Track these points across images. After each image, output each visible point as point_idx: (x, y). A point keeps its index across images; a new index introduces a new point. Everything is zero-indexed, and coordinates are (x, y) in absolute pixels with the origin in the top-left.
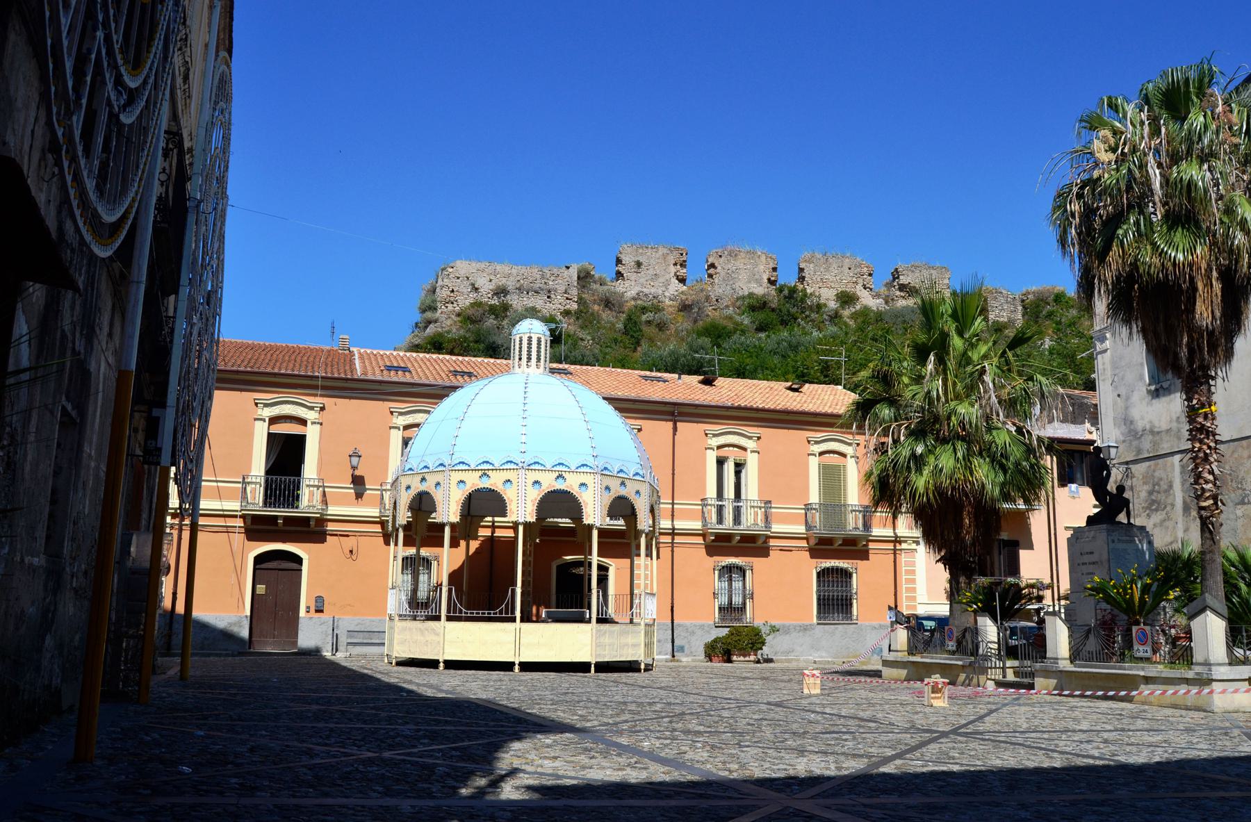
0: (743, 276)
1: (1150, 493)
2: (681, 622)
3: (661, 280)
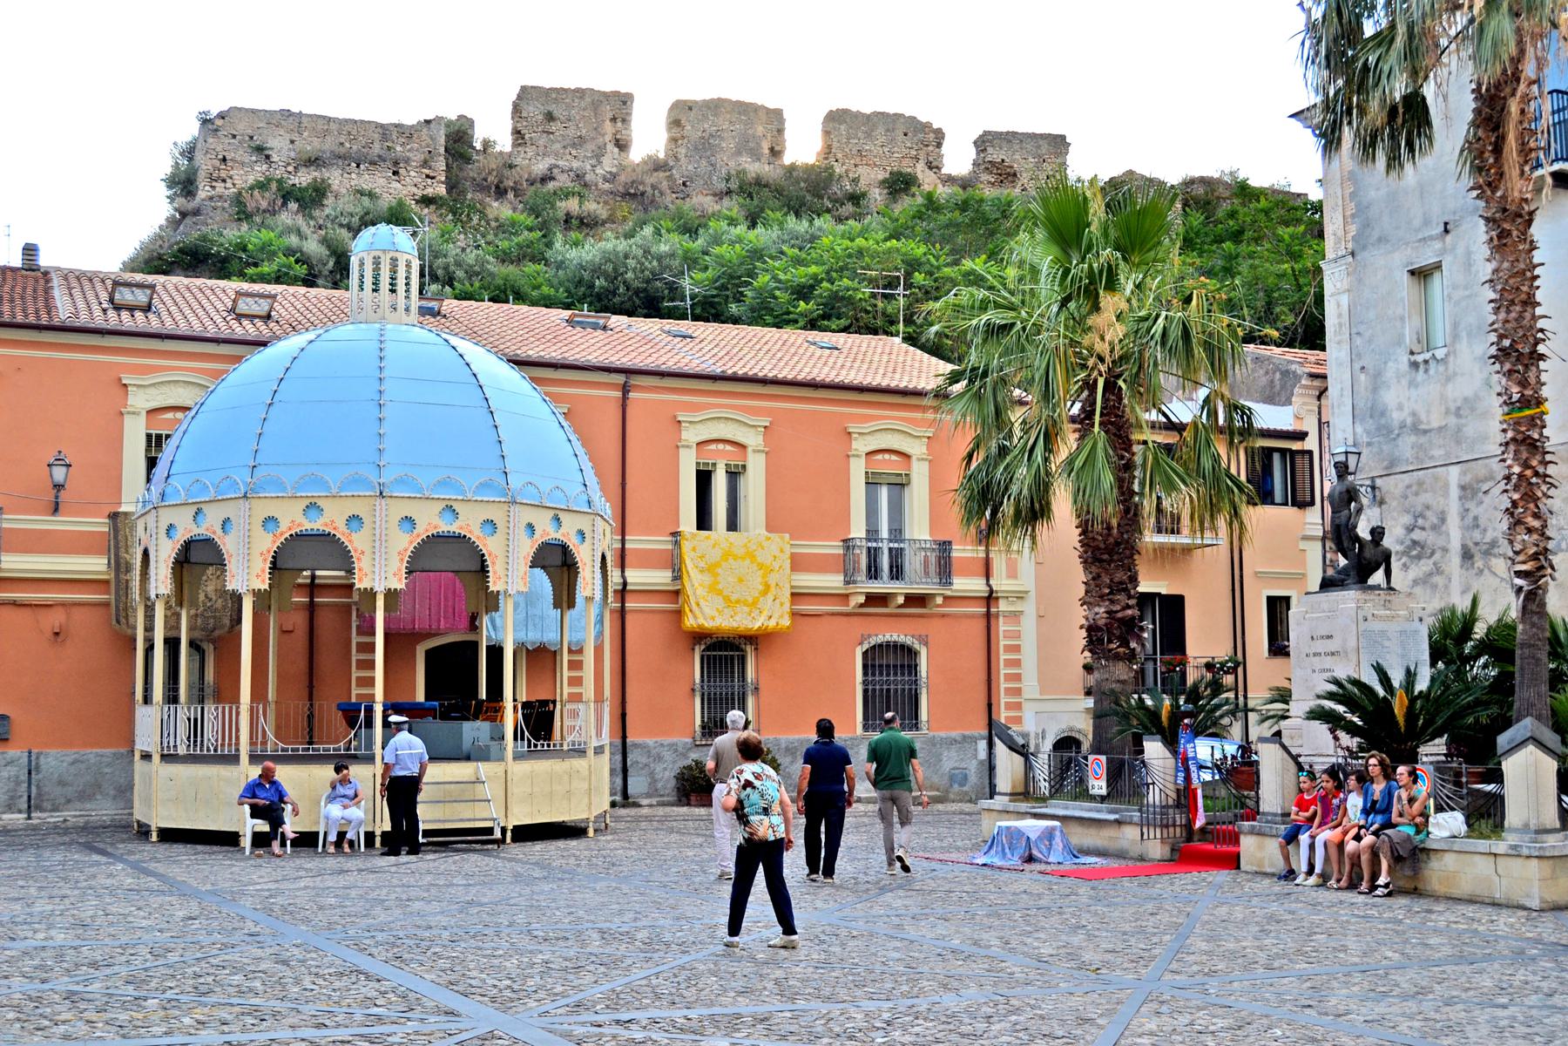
0: (729, 144)
1: (1410, 529)
2: (639, 740)
3: (590, 146)
